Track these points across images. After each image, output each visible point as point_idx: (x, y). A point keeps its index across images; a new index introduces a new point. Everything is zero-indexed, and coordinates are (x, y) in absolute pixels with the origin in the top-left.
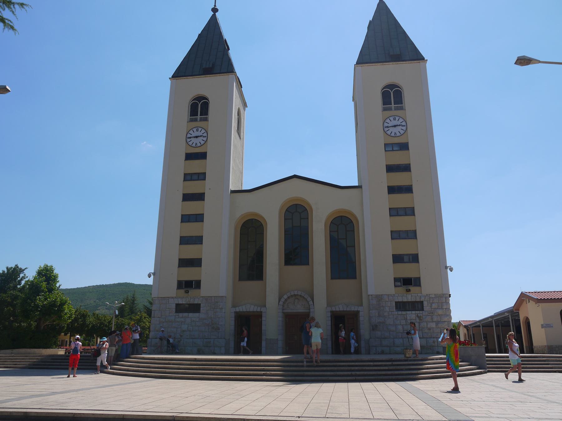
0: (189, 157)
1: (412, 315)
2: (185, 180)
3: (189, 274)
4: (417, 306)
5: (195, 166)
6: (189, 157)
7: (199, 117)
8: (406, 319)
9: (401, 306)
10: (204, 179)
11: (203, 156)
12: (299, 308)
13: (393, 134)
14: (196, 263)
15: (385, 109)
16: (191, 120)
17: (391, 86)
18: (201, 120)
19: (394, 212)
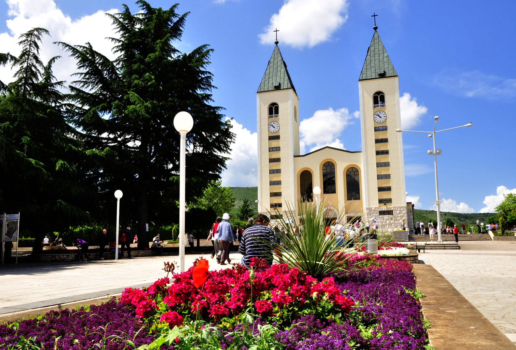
0: (271, 138)
1: (386, 217)
2: (269, 151)
3: (276, 200)
4: (389, 212)
5: (274, 143)
6: (271, 138)
7: (274, 115)
8: (384, 219)
9: (382, 213)
10: (280, 150)
11: (277, 137)
12: (331, 216)
13: (379, 122)
14: (278, 194)
15: (375, 107)
16: (270, 117)
17: (379, 93)
18: (275, 117)
19: (379, 165)
